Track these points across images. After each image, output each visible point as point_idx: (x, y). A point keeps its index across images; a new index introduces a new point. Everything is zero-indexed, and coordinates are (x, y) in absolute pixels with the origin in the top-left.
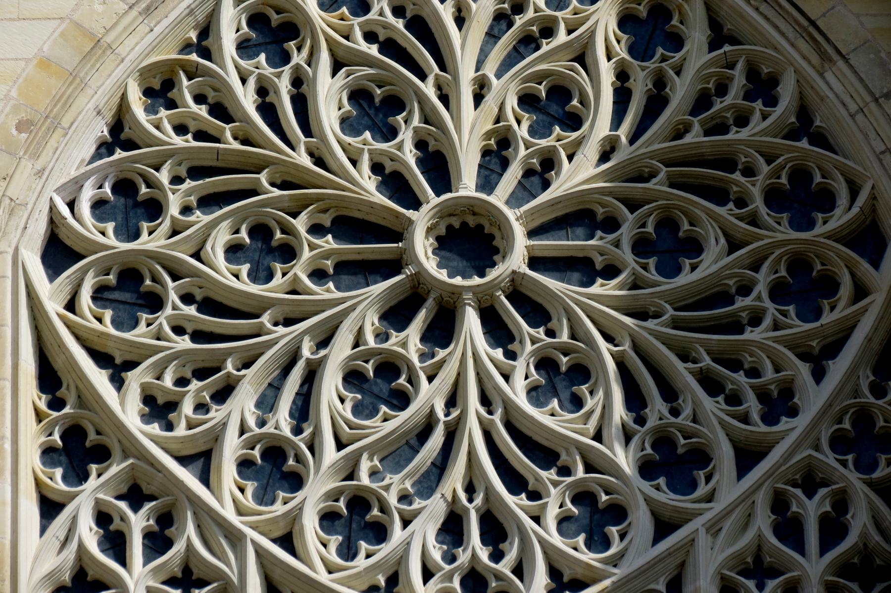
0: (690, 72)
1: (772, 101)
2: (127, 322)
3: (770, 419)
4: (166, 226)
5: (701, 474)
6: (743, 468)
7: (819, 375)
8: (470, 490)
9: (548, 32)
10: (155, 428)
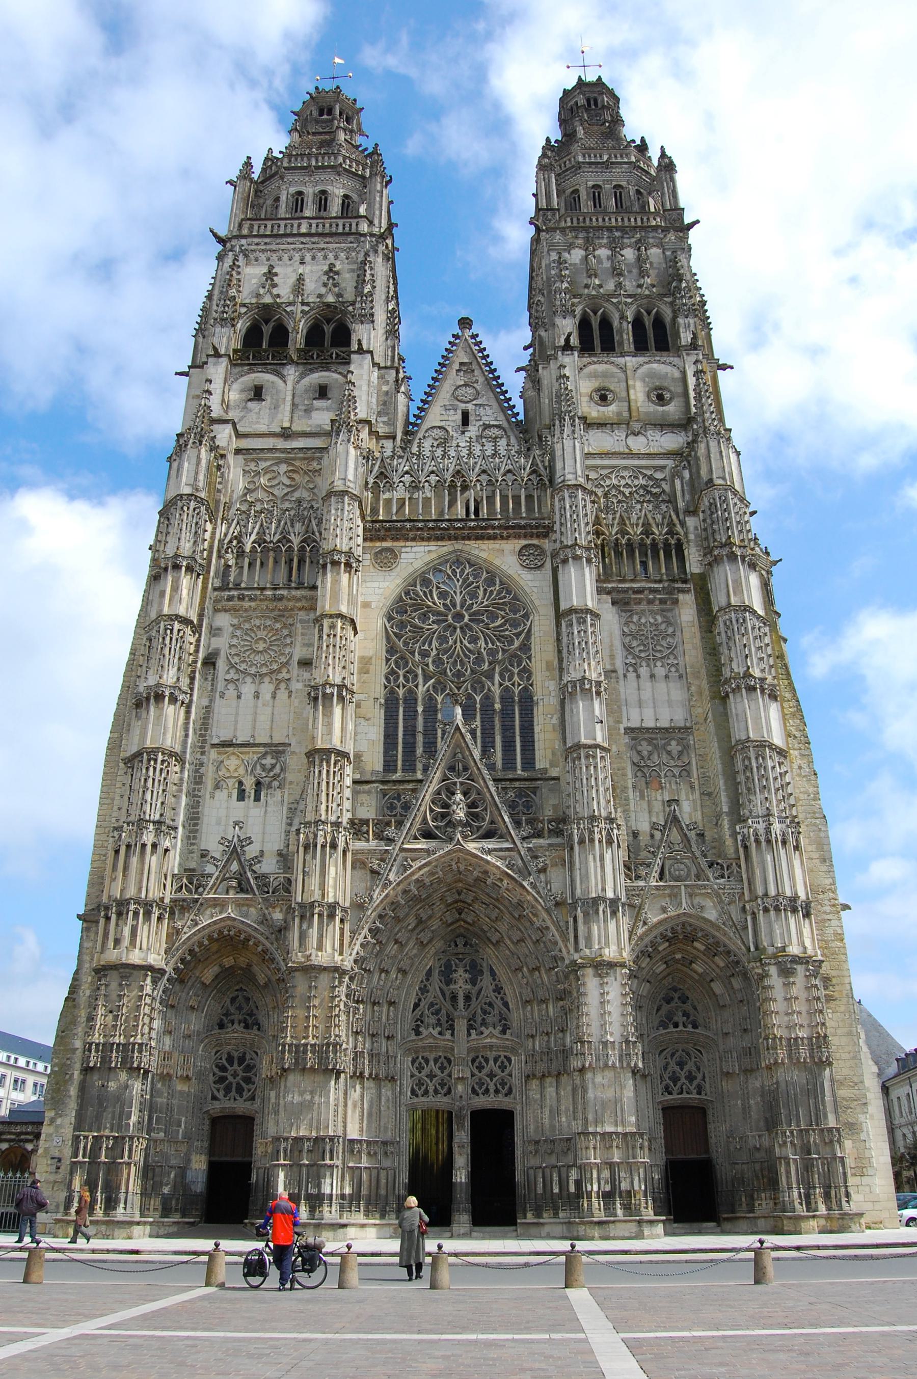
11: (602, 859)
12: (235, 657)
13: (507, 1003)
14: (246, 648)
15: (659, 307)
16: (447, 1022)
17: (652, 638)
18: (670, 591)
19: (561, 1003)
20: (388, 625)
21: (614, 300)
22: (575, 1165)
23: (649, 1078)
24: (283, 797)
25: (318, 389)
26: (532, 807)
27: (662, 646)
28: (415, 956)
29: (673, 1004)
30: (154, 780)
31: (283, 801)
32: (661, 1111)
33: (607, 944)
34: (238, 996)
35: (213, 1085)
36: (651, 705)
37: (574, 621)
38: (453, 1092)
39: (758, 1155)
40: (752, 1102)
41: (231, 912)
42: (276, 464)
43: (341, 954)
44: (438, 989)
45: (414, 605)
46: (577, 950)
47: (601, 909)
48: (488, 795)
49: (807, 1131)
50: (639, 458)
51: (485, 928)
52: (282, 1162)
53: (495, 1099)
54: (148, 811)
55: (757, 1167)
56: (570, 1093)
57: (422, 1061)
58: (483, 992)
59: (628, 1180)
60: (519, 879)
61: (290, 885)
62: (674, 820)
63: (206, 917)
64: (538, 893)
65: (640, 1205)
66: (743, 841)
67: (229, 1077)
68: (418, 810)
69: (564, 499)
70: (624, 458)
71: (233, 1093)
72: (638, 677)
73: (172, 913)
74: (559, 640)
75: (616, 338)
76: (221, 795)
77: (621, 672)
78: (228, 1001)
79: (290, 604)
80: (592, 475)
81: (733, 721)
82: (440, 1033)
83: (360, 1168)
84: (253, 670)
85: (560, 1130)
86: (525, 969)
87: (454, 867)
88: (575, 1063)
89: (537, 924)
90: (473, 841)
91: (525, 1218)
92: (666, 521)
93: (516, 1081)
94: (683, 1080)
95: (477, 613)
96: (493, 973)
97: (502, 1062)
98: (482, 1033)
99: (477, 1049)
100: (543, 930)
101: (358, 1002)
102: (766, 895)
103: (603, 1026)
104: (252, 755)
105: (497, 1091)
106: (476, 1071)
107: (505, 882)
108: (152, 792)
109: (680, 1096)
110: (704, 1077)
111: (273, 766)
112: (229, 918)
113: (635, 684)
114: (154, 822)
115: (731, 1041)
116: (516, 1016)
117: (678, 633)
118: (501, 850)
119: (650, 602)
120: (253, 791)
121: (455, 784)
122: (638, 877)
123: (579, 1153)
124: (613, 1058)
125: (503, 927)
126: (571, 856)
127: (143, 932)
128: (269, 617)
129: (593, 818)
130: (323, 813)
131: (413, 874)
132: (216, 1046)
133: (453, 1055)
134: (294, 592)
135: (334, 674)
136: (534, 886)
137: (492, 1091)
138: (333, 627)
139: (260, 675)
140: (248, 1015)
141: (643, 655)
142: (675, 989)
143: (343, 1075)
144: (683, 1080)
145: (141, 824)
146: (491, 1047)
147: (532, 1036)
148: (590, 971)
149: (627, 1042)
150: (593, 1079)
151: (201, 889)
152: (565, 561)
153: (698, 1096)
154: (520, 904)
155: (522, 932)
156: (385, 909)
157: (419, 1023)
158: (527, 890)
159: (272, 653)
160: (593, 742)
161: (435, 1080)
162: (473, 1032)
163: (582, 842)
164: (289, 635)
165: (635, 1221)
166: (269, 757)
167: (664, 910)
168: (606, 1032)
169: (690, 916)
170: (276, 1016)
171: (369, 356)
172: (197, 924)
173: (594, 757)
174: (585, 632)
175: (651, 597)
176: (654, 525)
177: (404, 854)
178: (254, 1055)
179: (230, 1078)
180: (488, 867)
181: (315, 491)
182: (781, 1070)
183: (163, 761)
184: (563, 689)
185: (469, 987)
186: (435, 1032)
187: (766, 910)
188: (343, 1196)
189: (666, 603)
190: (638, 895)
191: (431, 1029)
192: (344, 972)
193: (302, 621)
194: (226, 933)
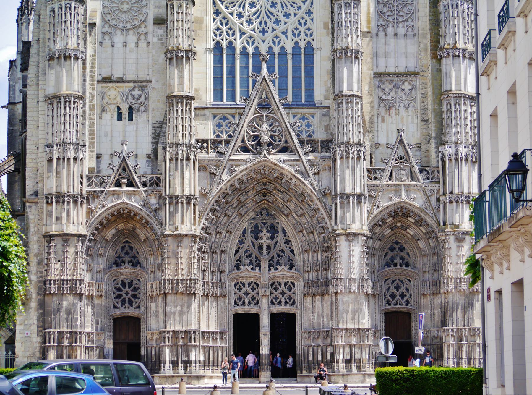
3: (298, 10)
6: (295, 16)
7: (304, 4)
10: (226, 10)
11: (353, 170)
12: (108, 15)
13: (293, 250)
14: (115, 9)
16: (256, 261)
17: (397, 6)
19: (326, 254)
22: (331, 345)
23: (377, 296)
26: (311, 126)
27: (404, 12)
28: (237, 222)
29: (395, 252)
30: (70, 115)
32: (383, 315)
33: (354, 222)
34: (125, 246)
35: (114, 299)
36: (393, 55)
37: (343, 5)
38: (260, 303)
39: (436, 341)
40: (436, 311)
41: (124, 199)
43: (194, 225)
44: (250, 242)
46: (336, 223)
47: (351, 201)
48: (283, 124)
49: (461, 329)
51: (280, 205)
52: (167, 343)
53: (285, 307)
54: (69, 137)
55: (435, 346)
56: (330, 305)
57: (241, 285)
58: (278, 244)
59: (360, 353)
60: (303, 179)
61: (160, 182)
62: (401, 142)
63: (109, 201)
64: (314, 188)
65: (365, 366)
66: (442, 157)
67: (123, 295)
68: (239, 134)
71: (127, 304)
72: (386, 35)
73: (88, 200)
74: (332, 12)
76: (107, 116)
77: (374, 32)
78: (120, 250)
81: (443, 75)
82: (252, 269)
83: (209, 347)
84: (121, 25)
85: (323, 326)
86: (304, 231)
87: (262, 171)
88: (333, 290)
89: (313, 207)
90: (274, 154)
91: (302, 373)
93: (298, 297)
94: (398, 297)
96: (284, 232)
97: (290, 286)
98: (277, 269)
99: (274, 278)
100: (316, 210)
101: (204, 253)
102: (451, 193)
103: (349, 269)
104: (125, 88)
105: (286, 303)
106: (274, 291)
107: (294, 179)
108: (70, 123)
109: (395, 306)
110: (411, 295)
111: (140, 96)
112: (123, 203)
113: (383, 40)
114: (73, 144)
115: (427, 275)
116: (298, 259)
118: (291, 160)
120: (127, 114)
121: (263, 116)
122: (375, 178)
123: (333, 339)
124: (354, 288)
125: (292, 206)
126: (335, 165)
127: (73, 213)
129: (348, 144)
130: (181, 138)
131: (237, 175)
132: (114, 277)
133: (260, 282)
135: (183, 42)
136: (311, 184)
137: (283, 302)
139: (127, 30)
140: (132, 257)
141: (390, 19)
142: (397, 243)
143: (197, 295)
144: (398, 297)
145: (64, 144)
146: (283, 277)
147: (308, 272)
148: (343, 238)
149: (363, 279)
150: (342, 299)
151: (104, 184)
153: (406, 307)
154: (302, 194)
155: (303, 210)
156: (219, 197)
157: (239, 262)
158: (307, 187)
159: (133, 12)
160: (351, 93)
161: (249, 296)
162: (272, 268)
163: (342, 158)
165: (362, 374)
166: (136, 89)
167: (391, 199)
168: (351, 273)
169: (406, 203)
170: (152, 259)
172: (103, 206)
173: (351, 103)
174: (350, 13)
177: (231, 162)
178: (138, 282)
179: (124, 296)
180: (283, 171)
182: (450, 295)
183: (74, 102)
184: (334, 51)
185: (270, 241)
186: (249, 268)
187: (451, 202)
188: (200, 362)
190: (375, 190)
191: (246, 267)
192: (197, 236)
194: (122, 211)
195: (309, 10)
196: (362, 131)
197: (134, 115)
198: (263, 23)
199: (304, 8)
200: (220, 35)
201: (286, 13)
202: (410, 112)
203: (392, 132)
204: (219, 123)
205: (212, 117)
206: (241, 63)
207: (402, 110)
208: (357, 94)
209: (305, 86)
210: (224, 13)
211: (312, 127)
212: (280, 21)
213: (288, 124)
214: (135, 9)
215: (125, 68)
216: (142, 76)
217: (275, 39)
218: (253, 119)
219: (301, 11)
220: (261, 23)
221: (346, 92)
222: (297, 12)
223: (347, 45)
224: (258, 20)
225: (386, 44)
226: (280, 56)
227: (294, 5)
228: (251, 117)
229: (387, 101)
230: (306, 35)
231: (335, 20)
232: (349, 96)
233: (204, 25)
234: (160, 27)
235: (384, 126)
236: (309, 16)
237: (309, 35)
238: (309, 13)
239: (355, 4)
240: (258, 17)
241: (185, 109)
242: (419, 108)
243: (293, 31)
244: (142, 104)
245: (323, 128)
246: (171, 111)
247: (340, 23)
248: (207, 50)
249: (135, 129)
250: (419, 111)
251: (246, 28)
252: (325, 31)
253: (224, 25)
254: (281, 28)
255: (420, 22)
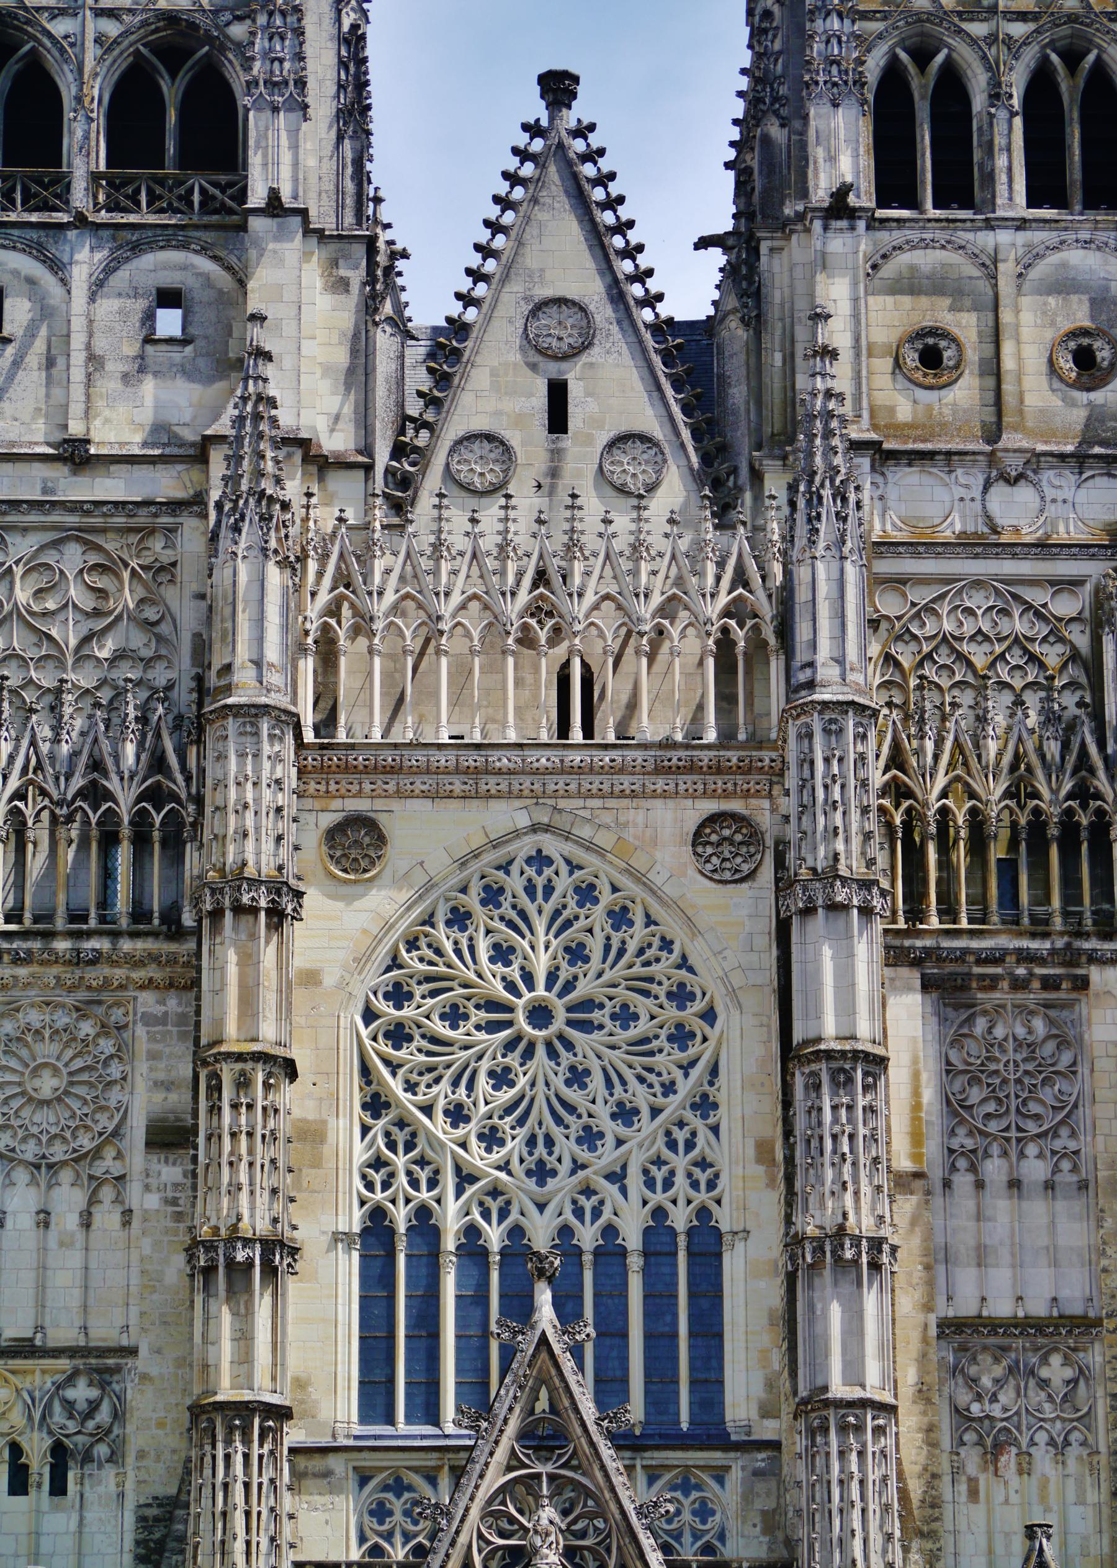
0: (636, 938)
1: (671, 952)
2: (397, 1047)
3: (665, 1095)
4: (414, 1005)
5: (636, 1119)
7: (686, 1075)
8: (540, 1124)
9: (577, 918)
10: (409, 1095)
15: (1099, 47)
17: (1019, 1081)
18: (1070, 957)
20: (364, 1033)
21: (978, 29)
24: (121, 1484)
25: (154, 292)
26: (713, 1513)
31: (121, 1495)
36: (1004, 1254)
37: (825, 1078)
42: (56, 544)
45: (429, 979)
48: (613, 1506)
50: (1014, 556)
68: (453, 1544)
69: (810, 736)
70: (976, 556)
72: (980, 1185)
74: (787, 1103)
75: (977, 155)
77: (936, 1174)
79: (119, 973)
80: (889, 605)
84: (30, 1150)
92: (1072, 759)
95: (588, 1004)
111: (94, 1406)
113: (971, 1204)
117: (1083, 1070)
119: (1019, 984)
121: (538, 1476)
128: (63, 1006)
134: (126, 945)
135: (252, 1209)
138: (243, 1083)
139: (50, 1166)
141: (993, 1127)
152: (808, 911)
159: (75, 1105)
160: (856, 1393)
164: (117, 1056)
166: (82, 1382)
171: (297, 220)
173: (859, 1429)
174: (850, 1108)
175: (1021, 971)
176: (1039, 773)
181: (165, 629)
184: (794, 1242)
189: (1057, 988)
193: (149, 1020)
195: (705, 1096)
196: (897, 1534)
197: (71, 1475)
198: (540, 1141)
199: (684, 1087)
200: (386, 1186)
201: (620, 1104)
202: (1072, 1465)
203: (1007, 1534)
204: (381, 1504)
205: (352, 1483)
206: (459, 1285)
207: (1043, 1458)
208: (877, 1397)
209: (692, 1368)
210: (399, 1104)
211: (718, 1517)
212: (601, 1135)
213: (630, 1508)
214: (81, 1090)
215: (41, 1305)
216: (104, 1332)
217: (582, 1200)
218: (502, 1489)
219: (674, 1100)
220: (531, 1142)
221: (838, 1389)
222: (660, 1100)
223: (840, 1220)
224: (522, 1133)
225: (979, 1217)
226: (602, 1259)
227: (652, 1078)
228: (494, 1480)
229: (987, 1422)
230: (695, 1185)
231: (797, 1133)
232: (851, 1404)
233: (327, 1150)
234: (171, 1158)
235: (978, 1512)
236: (705, 1117)
237: (703, 1186)
238: (704, 1105)
239: (866, 1074)
240: (521, 1122)
241: (256, 1451)
242: (1103, 1448)
243: (646, 1172)
244: (102, 1434)
245: (758, 1520)
246: (208, 1459)
247: (814, 1143)
248: (338, 1237)
249: (73, 1525)
250: (1103, 1458)
251: (478, 1157)
252: (761, 1169)
253: (401, 1148)
254: (604, 1162)
255: (1100, 1139)
